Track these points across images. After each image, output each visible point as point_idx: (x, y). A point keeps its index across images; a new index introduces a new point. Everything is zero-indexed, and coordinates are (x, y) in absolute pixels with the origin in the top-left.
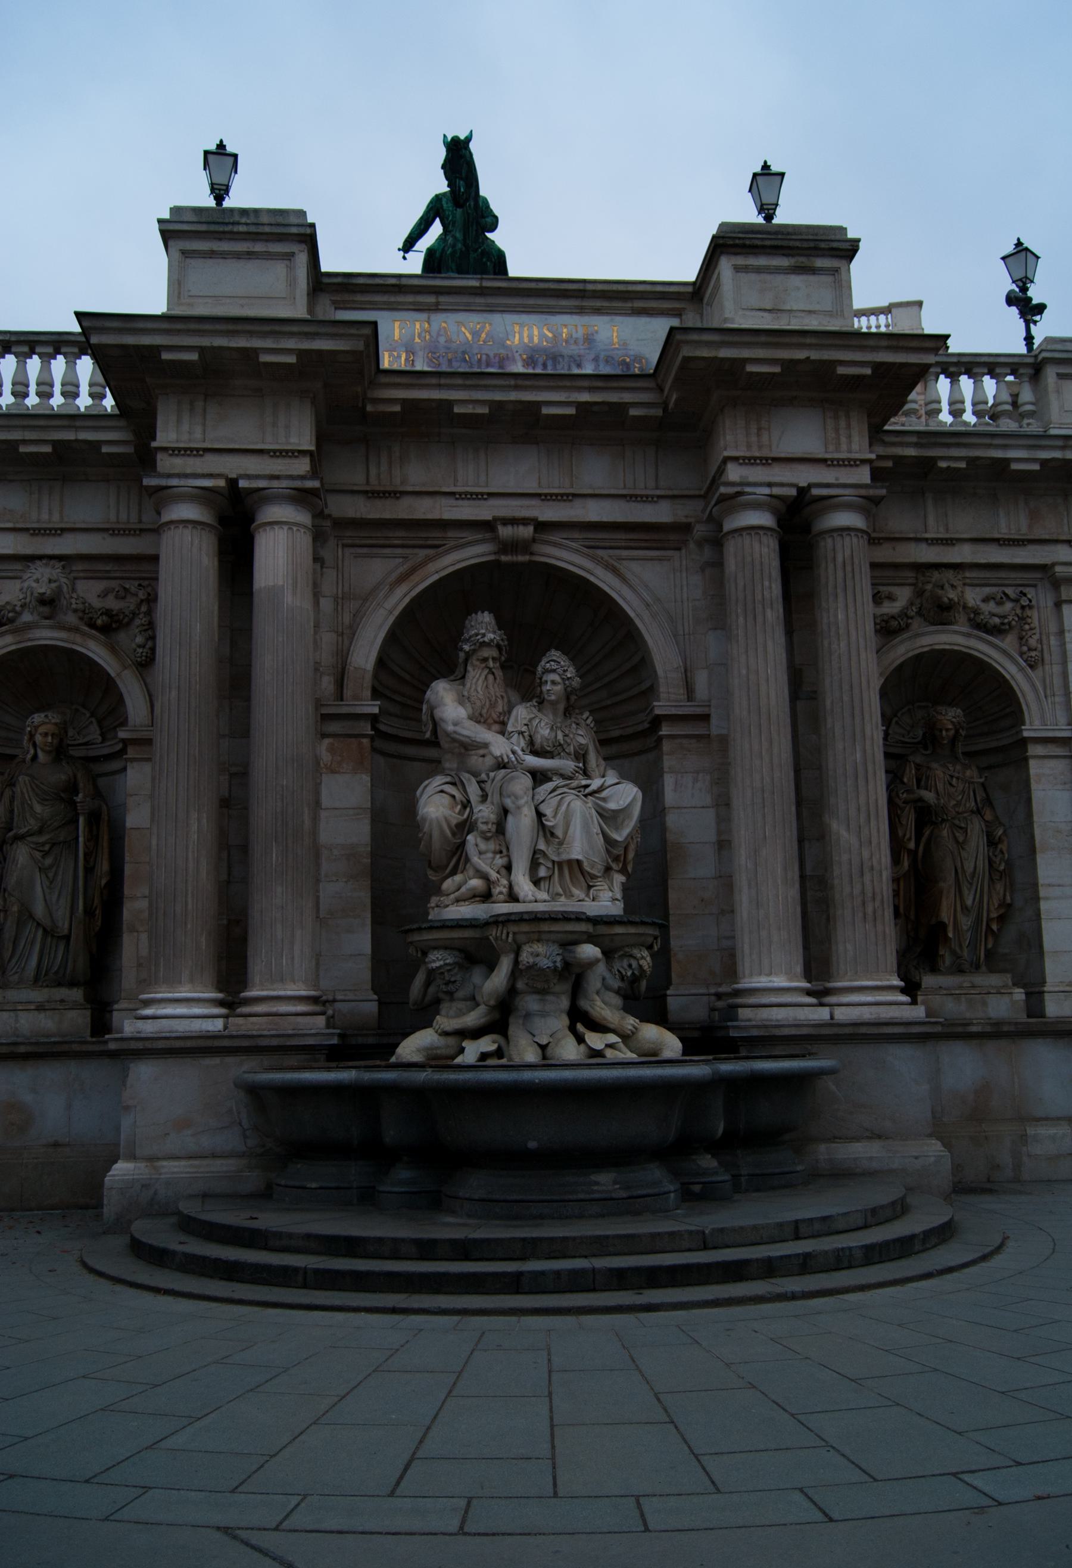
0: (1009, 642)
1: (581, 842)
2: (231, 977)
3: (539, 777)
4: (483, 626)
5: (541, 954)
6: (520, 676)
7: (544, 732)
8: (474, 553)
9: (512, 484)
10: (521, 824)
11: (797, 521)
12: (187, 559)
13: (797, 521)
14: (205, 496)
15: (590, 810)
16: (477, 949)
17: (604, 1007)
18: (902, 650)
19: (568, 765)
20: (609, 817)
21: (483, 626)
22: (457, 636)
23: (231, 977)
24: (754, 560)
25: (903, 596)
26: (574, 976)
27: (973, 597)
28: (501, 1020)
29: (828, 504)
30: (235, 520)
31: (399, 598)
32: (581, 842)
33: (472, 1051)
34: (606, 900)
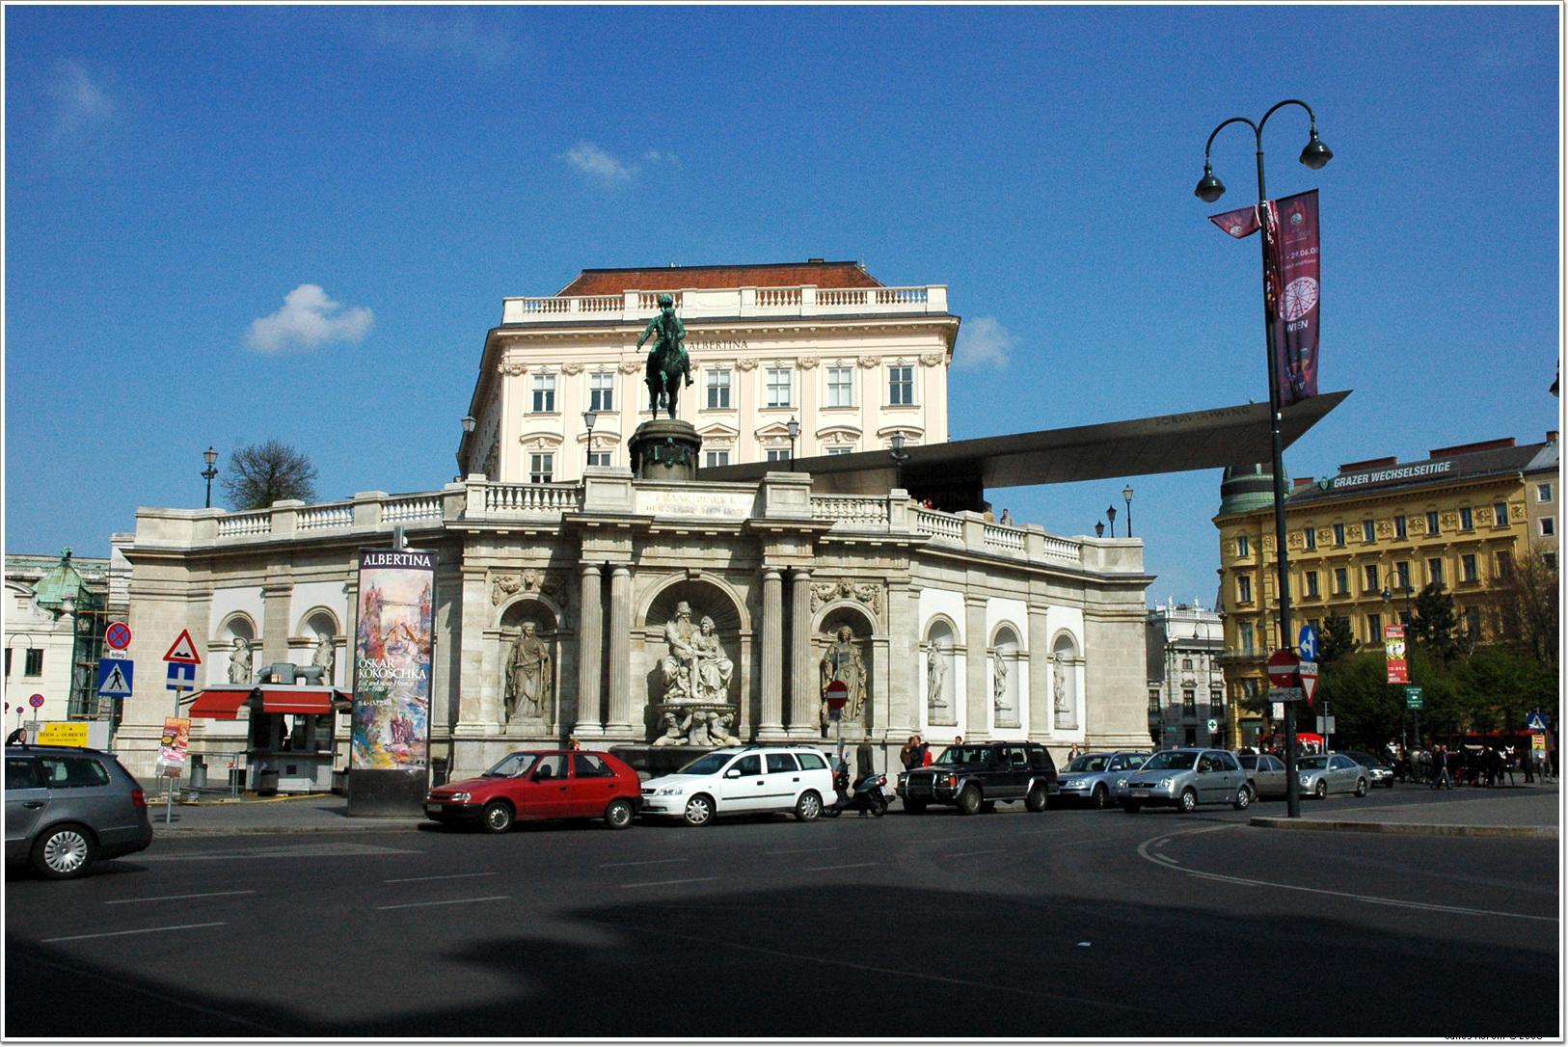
0: (870, 604)
1: (714, 681)
2: (604, 718)
3: (701, 658)
4: (684, 607)
5: (702, 716)
6: (695, 619)
7: (703, 644)
8: (681, 577)
9: (692, 557)
10: (696, 676)
11: (788, 577)
12: (592, 584)
13: (788, 577)
14: (598, 566)
15: (716, 667)
16: (681, 715)
17: (718, 730)
18: (831, 607)
19: (709, 654)
20: (723, 672)
21: (684, 607)
22: (676, 609)
23: (604, 718)
24: (774, 590)
25: (833, 586)
26: (709, 722)
27: (858, 587)
28: (686, 734)
29: (797, 571)
30: (607, 572)
31: (655, 593)
32: (714, 681)
33: (678, 742)
34: (721, 698)
